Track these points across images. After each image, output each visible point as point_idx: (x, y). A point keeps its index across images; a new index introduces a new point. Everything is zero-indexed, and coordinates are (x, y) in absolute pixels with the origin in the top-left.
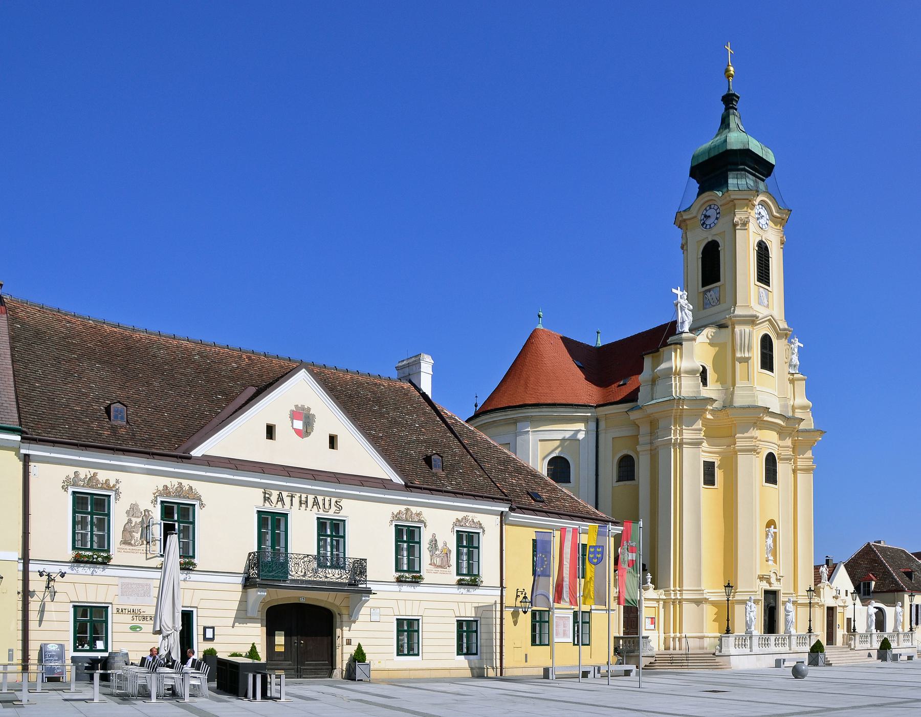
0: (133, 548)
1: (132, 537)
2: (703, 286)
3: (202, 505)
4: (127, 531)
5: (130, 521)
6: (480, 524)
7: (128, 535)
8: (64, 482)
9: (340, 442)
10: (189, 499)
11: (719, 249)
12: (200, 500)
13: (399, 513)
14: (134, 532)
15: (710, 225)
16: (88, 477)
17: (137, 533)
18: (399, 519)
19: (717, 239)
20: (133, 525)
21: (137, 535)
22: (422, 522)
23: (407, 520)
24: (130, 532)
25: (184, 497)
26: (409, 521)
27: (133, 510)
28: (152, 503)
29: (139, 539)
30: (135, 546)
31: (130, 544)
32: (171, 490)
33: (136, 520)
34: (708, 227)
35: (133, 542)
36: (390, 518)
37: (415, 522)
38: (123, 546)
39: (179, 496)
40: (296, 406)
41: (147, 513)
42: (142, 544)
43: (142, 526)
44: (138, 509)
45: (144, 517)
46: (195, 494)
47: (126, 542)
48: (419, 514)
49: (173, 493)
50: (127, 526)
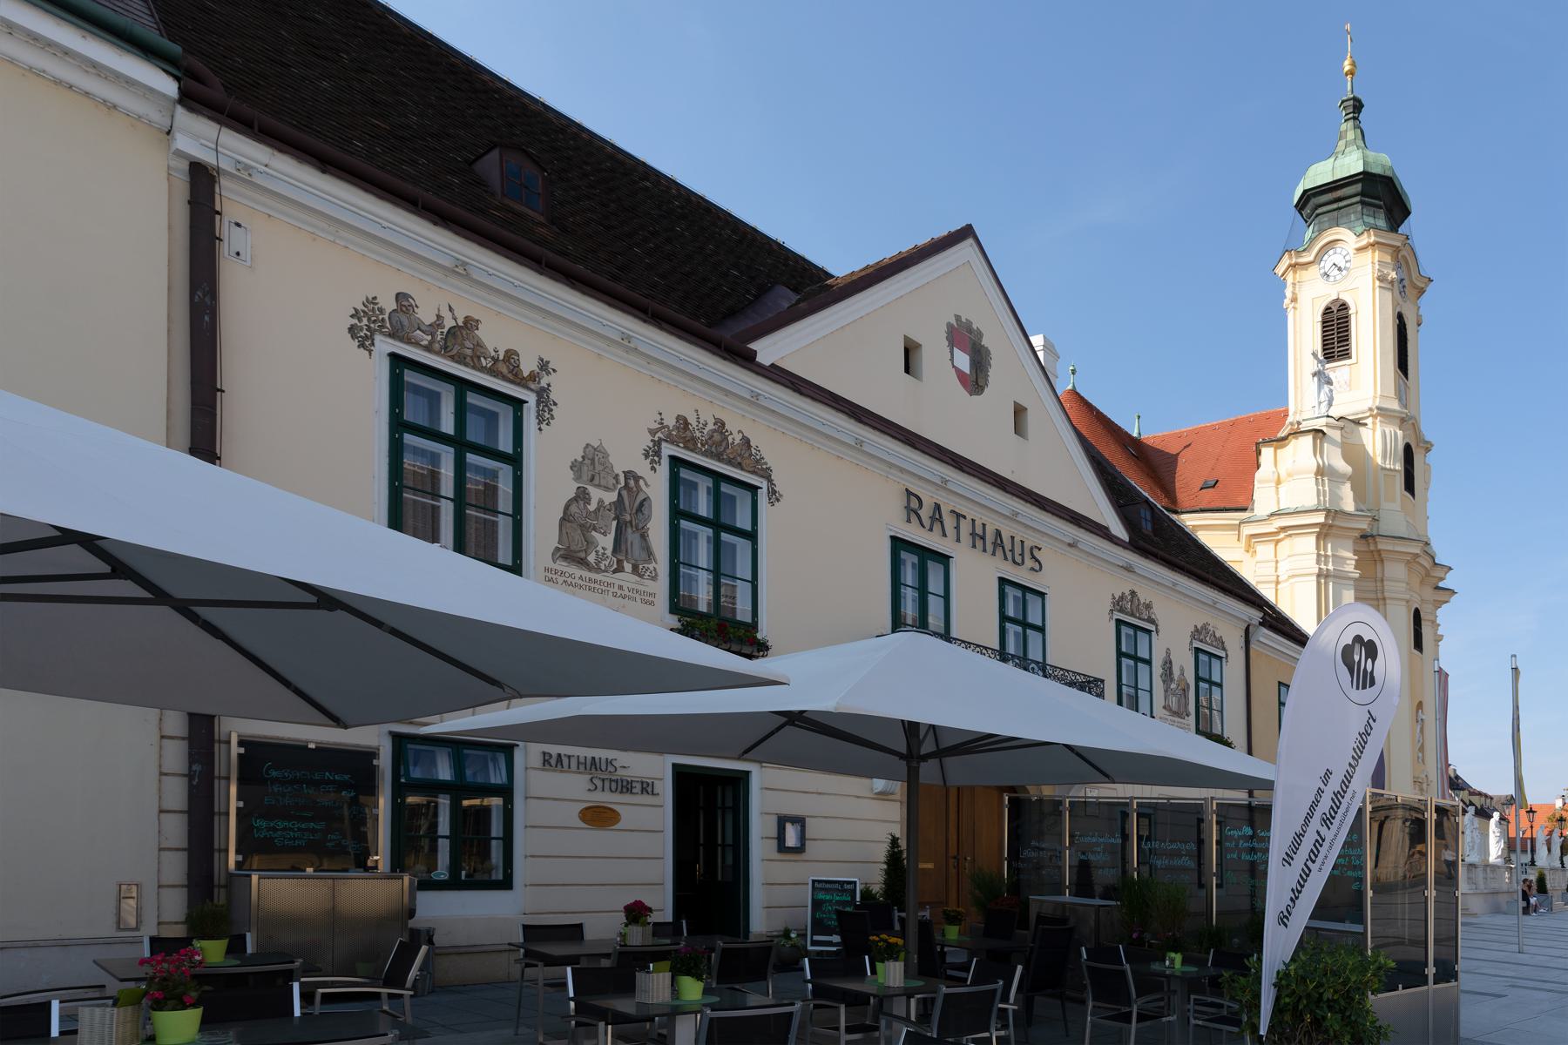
0: (594, 576)
1: (590, 544)
7: (577, 535)
9: (1032, 419)
10: (742, 469)
11: (1350, 312)
13: (1122, 597)
14: (595, 529)
17: (605, 534)
18: (1121, 611)
19: (1346, 297)
21: (606, 542)
22: (1152, 621)
23: (1132, 615)
24: (585, 529)
25: (730, 462)
26: (1135, 617)
28: (647, 456)
29: (609, 552)
30: (598, 570)
31: (582, 562)
32: (698, 434)
35: (591, 558)
36: (1109, 606)
37: (1140, 619)
38: (561, 566)
39: (718, 457)
40: (958, 318)
41: (632, 483)
43: (617, 518)
45: (624, 493)
46: (757, 461)
48: (1148, 606)
49: (703, 445)
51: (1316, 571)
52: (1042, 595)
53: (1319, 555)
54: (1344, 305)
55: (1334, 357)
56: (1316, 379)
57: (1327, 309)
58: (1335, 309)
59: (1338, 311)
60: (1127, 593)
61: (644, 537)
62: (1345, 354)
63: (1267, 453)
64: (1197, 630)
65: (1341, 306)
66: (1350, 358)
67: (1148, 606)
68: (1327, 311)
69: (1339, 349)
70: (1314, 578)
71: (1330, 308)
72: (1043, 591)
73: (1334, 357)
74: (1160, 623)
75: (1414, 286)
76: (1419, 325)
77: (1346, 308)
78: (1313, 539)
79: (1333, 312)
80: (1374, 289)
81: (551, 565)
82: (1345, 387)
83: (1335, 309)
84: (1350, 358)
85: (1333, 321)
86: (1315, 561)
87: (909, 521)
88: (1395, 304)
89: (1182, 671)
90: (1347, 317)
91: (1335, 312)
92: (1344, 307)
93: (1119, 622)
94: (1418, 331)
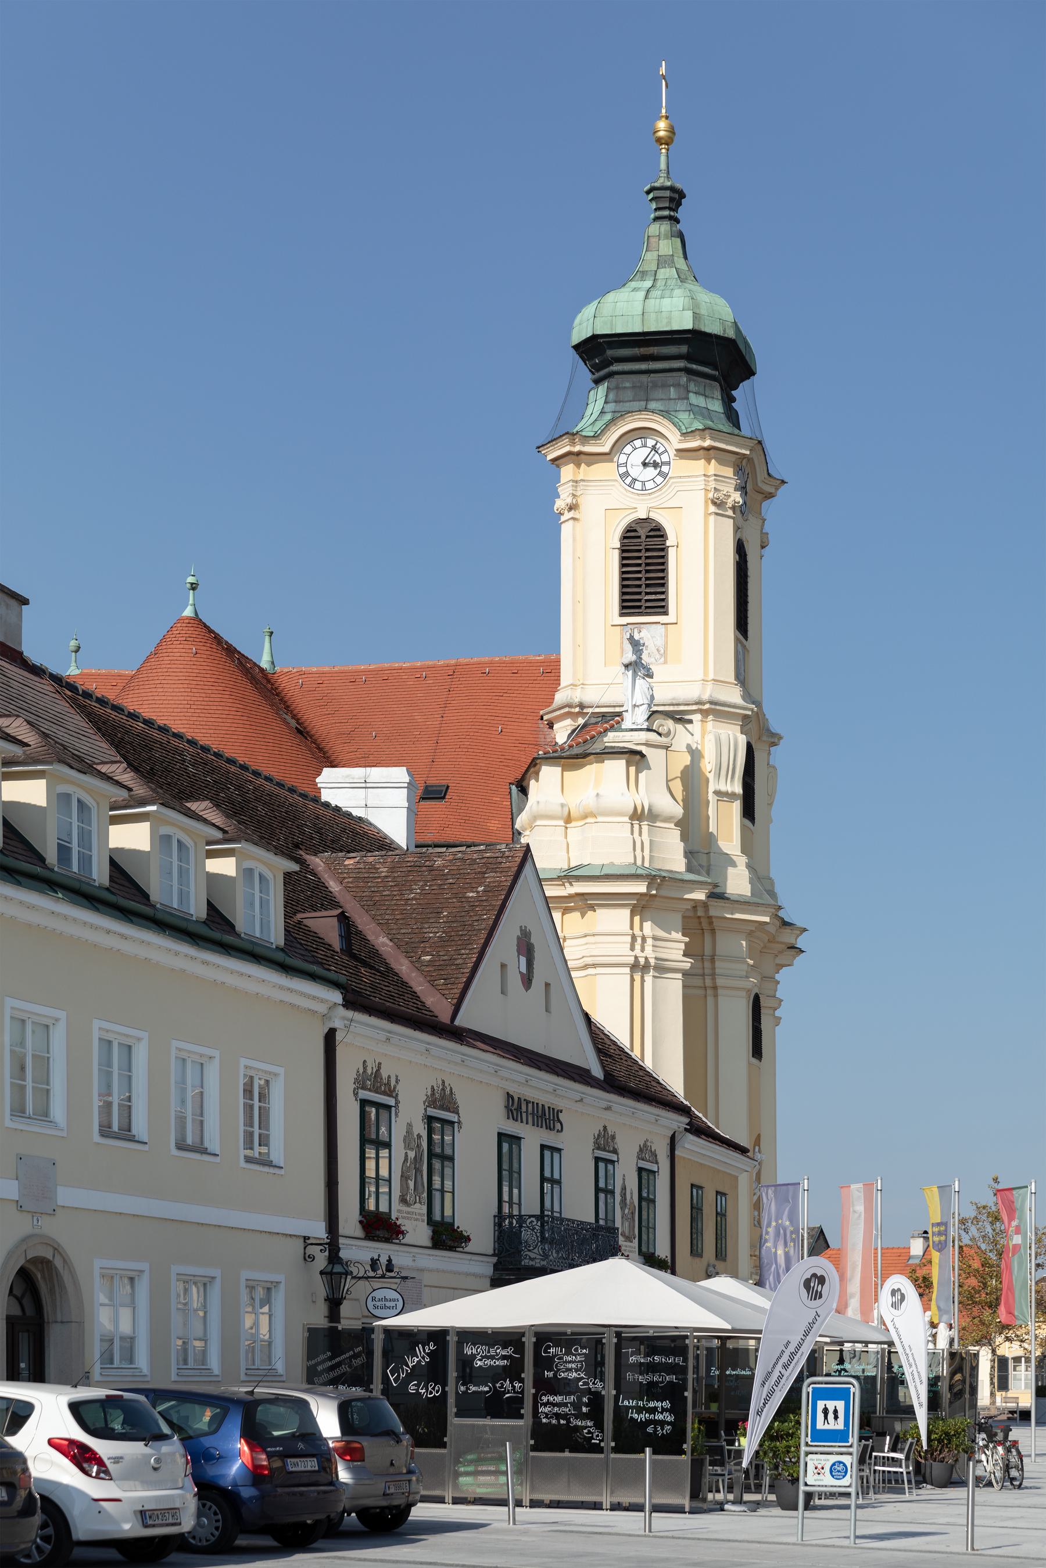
1: (408, 1188)
2: (622, 615)
3: (459, 1122)
4: (404, 1177)
5: (406, 1155)
6: (656, 1156)
8: (354, 1083)
11: (668, 543)
12: (458, 1113)
15: (643, 483)
16: (374, 1070)
20: (408, 1164)
21: (411, 1184)
22: (615, 1151)
23: (604, 1150)
27: (409, 1138)
33: (412, 1154)
34: (638, 485)
36: (591, 1146)
42: (415, 1203)
43: (415, 1168)
44: (412, 1134)
47: (403, 1200)
50: (404, 1168)
51: (631, 960)
52: (559, 1150)
53: (634, 938)
54: (659, 530)
55: (640, 607)
56: (630, 673)
57: (628, 531)
58: (642, 532)
59: (647, 537)
60: (602, 1129)
61: (422, 1176)
62: (661, 608)
63: (549, 774)
64: (641, 1150)
65: (652, 530)
66: (666, 613)
67: (613, 1137)
68: (630, 534)
69: (648, 590)
70: (627, 970)
71: (635, 531)
72: (559, 1147)
73: (640, 607)
74: (620, 1151)
75: (760, 492)
76: (763, 547)
77: (662, 536)
78: (626, 912)
79: (639, 537)
80: (707, 514)
81: (401, 1208)
82: (658, 656)
83: (642, 532)
84: (666, 613)
85: (640, 551)
86: (629, 946)
87: (508, 1118)
88: (737, 529)
89: (632, 1193)
90: (663, 550)
91: (643, 537)
92: (657, 532)
93: (597, 1160)
94: (762, 557)
